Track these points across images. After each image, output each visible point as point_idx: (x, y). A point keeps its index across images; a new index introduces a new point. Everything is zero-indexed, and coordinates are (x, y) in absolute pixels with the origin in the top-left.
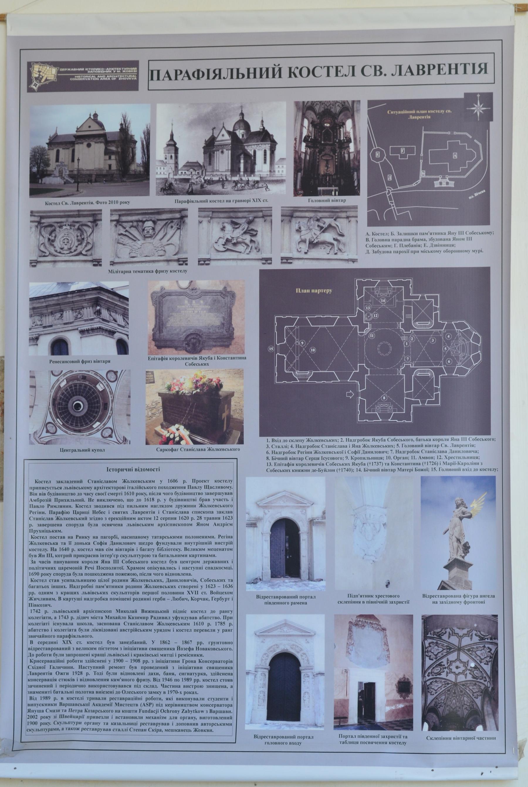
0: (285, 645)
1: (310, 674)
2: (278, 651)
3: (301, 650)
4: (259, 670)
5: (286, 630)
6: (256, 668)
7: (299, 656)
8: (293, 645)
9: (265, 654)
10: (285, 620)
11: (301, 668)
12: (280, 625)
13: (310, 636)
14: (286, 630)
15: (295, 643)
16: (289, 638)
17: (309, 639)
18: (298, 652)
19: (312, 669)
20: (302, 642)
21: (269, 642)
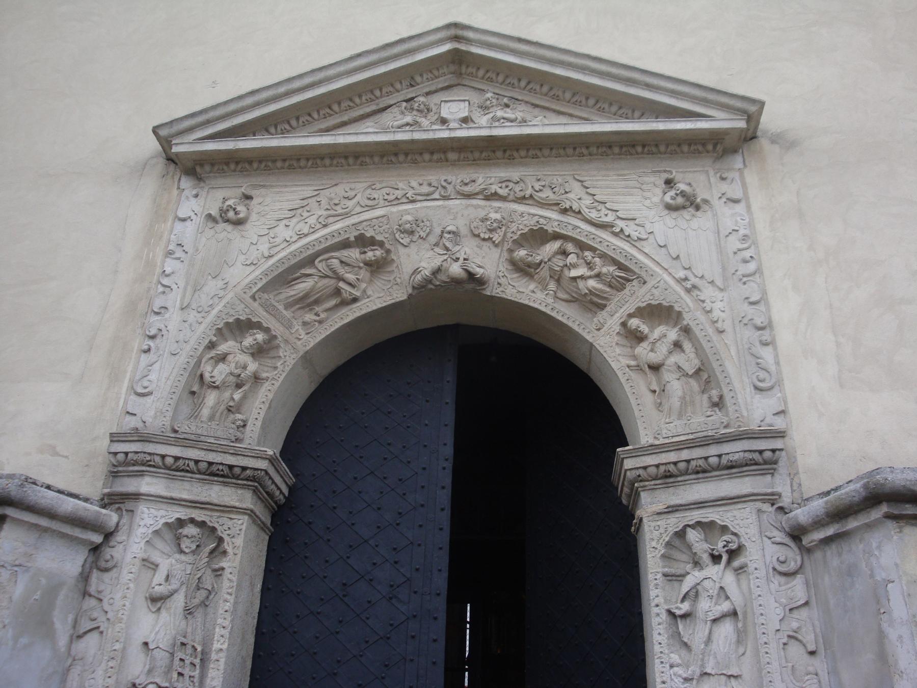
0: (448, 236)
1: (744, 522)
2: (377, 296)
3: (625, 275)
4: (149, 485)
5: (459, 113)
6: (122, 466)
7: (603, 340)
8: (538, 236)
9: (241, 327)
10: (456, 31)
11: (630, 463)
12: (408, 76)
13: (718, 147)
14: (459, 113)
15: (552, 219)
16: (489, 177)
17: (696, 177)
18: (593, 304)
19: (765, 463)
20: (630, 205)
21: (285, 221)
